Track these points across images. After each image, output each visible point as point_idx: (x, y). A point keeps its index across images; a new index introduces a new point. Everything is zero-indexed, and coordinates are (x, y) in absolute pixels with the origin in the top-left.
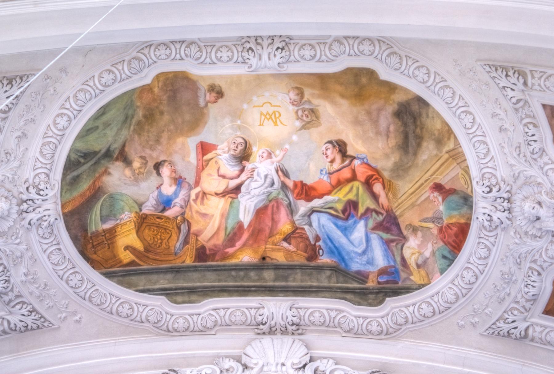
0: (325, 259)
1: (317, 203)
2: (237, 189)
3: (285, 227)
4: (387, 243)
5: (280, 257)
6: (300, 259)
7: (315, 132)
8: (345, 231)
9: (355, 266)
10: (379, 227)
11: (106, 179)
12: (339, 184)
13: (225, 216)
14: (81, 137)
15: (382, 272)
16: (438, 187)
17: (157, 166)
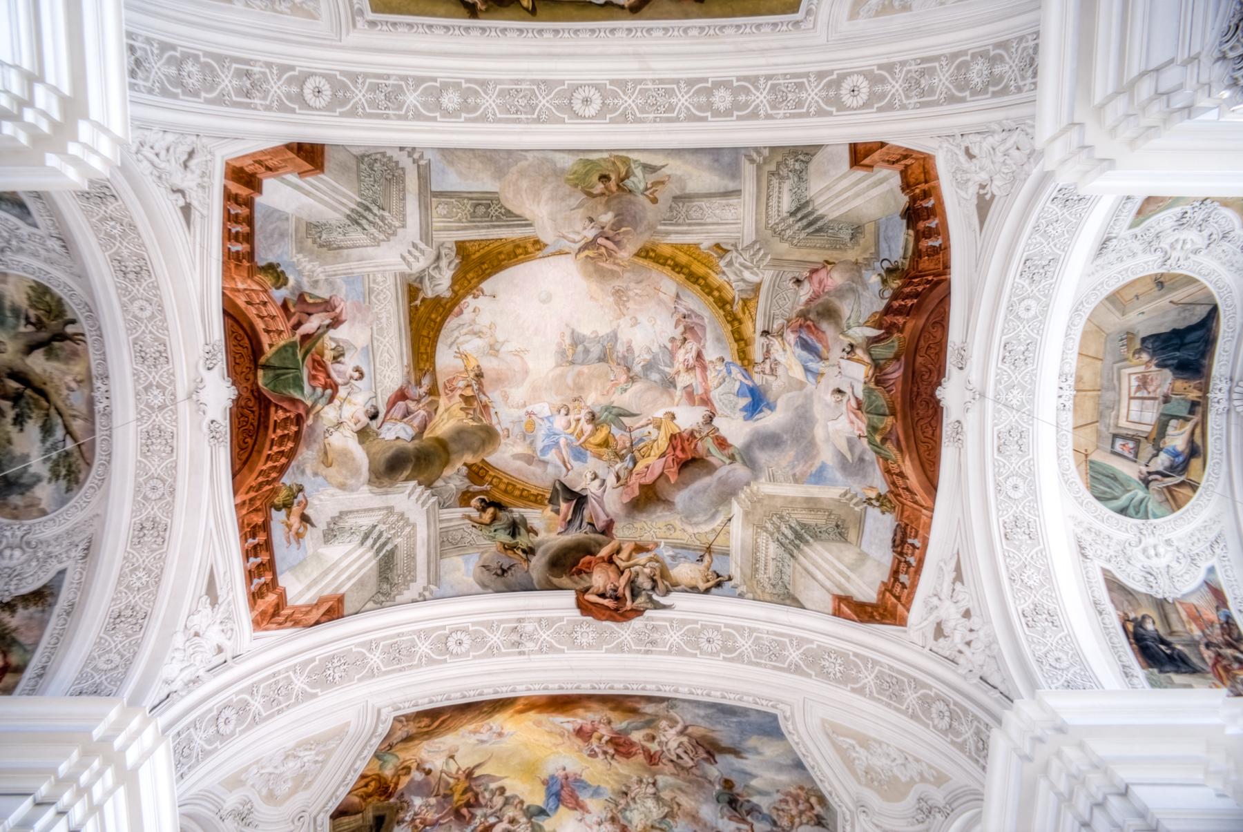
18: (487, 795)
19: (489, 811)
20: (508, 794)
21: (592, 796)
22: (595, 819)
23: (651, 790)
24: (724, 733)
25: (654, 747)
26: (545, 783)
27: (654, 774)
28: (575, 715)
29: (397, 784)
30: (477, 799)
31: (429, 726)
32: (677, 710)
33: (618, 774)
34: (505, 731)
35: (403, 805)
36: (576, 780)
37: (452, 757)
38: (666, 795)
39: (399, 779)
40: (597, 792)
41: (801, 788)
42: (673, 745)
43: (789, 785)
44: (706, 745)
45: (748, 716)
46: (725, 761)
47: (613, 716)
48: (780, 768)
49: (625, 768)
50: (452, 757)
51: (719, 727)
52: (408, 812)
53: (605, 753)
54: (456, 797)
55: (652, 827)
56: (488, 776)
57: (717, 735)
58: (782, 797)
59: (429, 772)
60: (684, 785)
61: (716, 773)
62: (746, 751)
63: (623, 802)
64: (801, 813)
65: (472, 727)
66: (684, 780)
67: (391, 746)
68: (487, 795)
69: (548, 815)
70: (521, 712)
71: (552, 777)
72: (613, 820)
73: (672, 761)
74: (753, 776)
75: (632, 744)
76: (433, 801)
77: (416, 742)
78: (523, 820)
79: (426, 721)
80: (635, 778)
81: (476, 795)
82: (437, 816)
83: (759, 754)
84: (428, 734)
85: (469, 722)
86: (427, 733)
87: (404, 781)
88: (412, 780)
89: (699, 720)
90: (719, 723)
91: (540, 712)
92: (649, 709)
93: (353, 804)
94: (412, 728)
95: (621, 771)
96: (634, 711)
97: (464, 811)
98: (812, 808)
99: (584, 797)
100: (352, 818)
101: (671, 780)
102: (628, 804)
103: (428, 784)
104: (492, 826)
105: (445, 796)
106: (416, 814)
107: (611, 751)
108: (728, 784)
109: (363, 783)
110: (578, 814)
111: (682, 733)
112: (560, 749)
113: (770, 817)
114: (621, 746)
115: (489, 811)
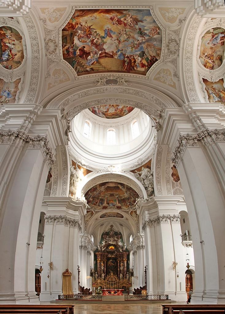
0: (3, 53)
1: (9, 52)
2: (10, 44)
3: (6, 49)
4: (6, 60)
5: (3, 48)
6: (3, 50)
7: (17, 52)
8: (7, 55)
9: (3, 56)
10: (7, 59)
11: (9, 31)
12: (12, 55)
13: (6, 42)
14: (13, 28)
15: (3, 59)
16: (12, 66)
17: (11, 36)
18: (93, 33)
19: (94, 36)
20: (97, 33)
21: (113, 34)
22: (114, 39)
23: (125, 32)
24: (139, 17)
25: (126, 22)
26: (104, 31)
27: (125, 29)
28: (110, 14)
29: (75, 27)
30: (91, 33)
31: (82, 13)
32: (130, 12)
33: (118, 29)
34: (97, 17)
35: (77, 32)
36: (110, 30)
37: (86, 23)
38: (128, 33)
39: (76, 26)
40: (114, 33)
41: (155, 27)
42: (129, 21)
43: (152, 27)
44: (136, 20)
45: (144, 11)
46: (140, 23)
47: (117, 14)
48: (150, 23)
49: (120, 27)
50: (86, 23)
51: (138, 15)
52: (77, 33)
53: (116, 24)
54: (87, 32)
55: (125, 40)
56: (93, 28)
57: (137, 17)
58: (151, 30)
59: (82, 25)
60: (131, 31)
61: (138, 27)
62: (144, 21)
63: (119, 35)
64: (155, 32)
65: (90, 15)
66: (131, 29)
67: (74, 17)
68: (93, 33)
69: (105, 38)
70: (100, 13)
71: (106, 29)
72: (117, 39)
73: (129, 25)
74: (145, 26)
75: (121, 21)
76: (82, 32)
77: (79, 17)
78: (100, 39)
79: (81, 12)
80: (122, 30)
81: (91, 32)
82: (83, 36)
83: (146, 21)
84: (82, 16)
85: (90, 14)
86: (81, 15)
87: (77, 26)
88: (78, 26)
89: (134, 14)
90: (138, 14)
91: (104, 13)
92: (125, 12)
93: (66, 29)
94: (78, 13)
95: (119, 28)
96: (122, 13)
97: (89, 35)
98: (157, 31)
99: (112, 34)
100: (66, 32)
101: (129, 30)
102: (120, 36)
103: (81, 28)
104: (94, 39)
105: (85, 31)
106: (79, 34)
107: (117, 23)
108: (140, 29)
109: (69, 24)
110: (110, 38)
111: (131, 18)
112: (107, 23)
113: (148, 35)
114: (119, 22)
115: (94, 36)
